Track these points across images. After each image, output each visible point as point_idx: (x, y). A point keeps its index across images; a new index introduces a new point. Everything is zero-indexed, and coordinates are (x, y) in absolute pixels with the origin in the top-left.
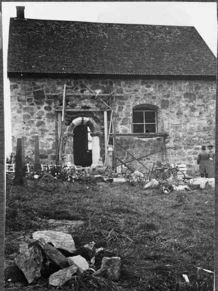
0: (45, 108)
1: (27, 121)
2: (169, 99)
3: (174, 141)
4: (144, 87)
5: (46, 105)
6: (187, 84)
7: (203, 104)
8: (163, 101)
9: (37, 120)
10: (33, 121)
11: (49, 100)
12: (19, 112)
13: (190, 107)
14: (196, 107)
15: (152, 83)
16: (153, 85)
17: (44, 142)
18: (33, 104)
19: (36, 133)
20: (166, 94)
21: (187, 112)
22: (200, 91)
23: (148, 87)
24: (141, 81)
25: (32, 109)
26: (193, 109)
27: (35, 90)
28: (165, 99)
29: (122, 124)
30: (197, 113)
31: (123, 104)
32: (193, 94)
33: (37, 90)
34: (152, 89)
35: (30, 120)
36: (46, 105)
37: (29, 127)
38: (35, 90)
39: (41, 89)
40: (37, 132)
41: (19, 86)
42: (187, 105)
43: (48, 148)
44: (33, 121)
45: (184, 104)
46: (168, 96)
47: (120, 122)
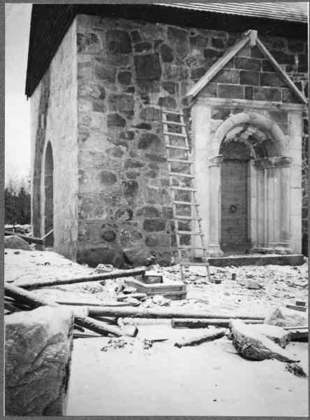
0: (161, 101)
1: (118, 131)
5: (163, 94)
9: (141, 131)
10: (132, 135)
11: (170, 80)
12: (98, 108)
17: (157, 188)
18: (132, 90)
19: (138, 165)
27: (140, 54)
33: (144, 52)
35: (124, 130)
36: (163, 94)
37: (123, 148)
38: (140, 54)
39: (152, 51)
40: (142, 162)
41: (99, 37)
43: (165, 205)
44: (132, 135)
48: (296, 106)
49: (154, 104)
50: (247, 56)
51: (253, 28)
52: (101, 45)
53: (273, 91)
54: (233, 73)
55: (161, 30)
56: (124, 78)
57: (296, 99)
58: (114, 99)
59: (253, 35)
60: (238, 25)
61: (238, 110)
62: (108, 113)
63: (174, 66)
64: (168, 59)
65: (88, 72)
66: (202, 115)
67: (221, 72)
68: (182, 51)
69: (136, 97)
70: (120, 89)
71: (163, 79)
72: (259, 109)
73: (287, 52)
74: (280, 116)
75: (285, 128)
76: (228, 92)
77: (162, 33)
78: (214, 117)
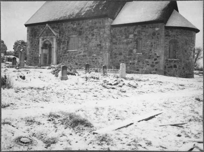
0: (37, 39)
2: (82, 30)
3: (84, 52)
4: (72, 25)
6: (91, 21)
7: (98, 31)
8: (80, 31)
12: (29, 41)
13: (91, 34)
14: (94, 33)
15: (75, 23)
16: (75, 24)
18: (33, 37)
20: (81, 27)
21: (90, 37)
22: (96, 25)
23: (74, 25)
24: (70, 22)
25: (33, 39)
26: (93, 35)
28: (80, 30)
29: (62, 44)
30: (94, 37)
31: (63, 34)
32: (93, 27)
34: (75, 26)
42: (90, 33)
45: (88, 32)
46: (82, 29)
47: (62, 43)
48: (54, 37)
49: (36, 39)
50: (47, 28)
51: (47, 24)
52: (30, 31)
53: (51, 34)
54: (45, 32)
55: (37, 27)
56: (32, 36)
57: (54, 35)
58: (31, 39)
59: (47, 24)
60: (44, 24)
61: (45, 39)
62: (30, 41)
63: (39, 32)
64: (38, 31)
65: (28, 36)
66: (40, 40)
67: (43, 33)
68: (40, 29)
69: (34, 38)
70: (31, 37)
71: (37, 35)
72: (48, 38)
73: (56, 26)
74: (52, 39)
75: (53, 41)
76: (44, 35)
77: (37, 27)
78: (42, 40)
